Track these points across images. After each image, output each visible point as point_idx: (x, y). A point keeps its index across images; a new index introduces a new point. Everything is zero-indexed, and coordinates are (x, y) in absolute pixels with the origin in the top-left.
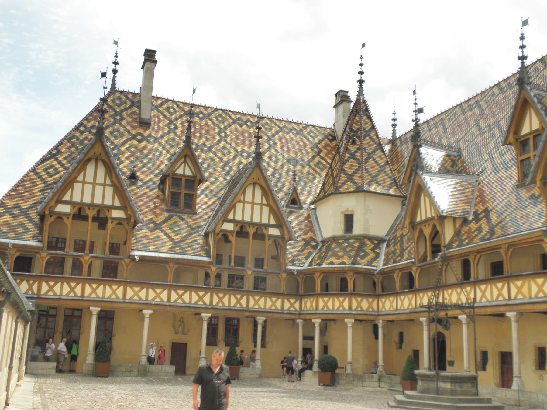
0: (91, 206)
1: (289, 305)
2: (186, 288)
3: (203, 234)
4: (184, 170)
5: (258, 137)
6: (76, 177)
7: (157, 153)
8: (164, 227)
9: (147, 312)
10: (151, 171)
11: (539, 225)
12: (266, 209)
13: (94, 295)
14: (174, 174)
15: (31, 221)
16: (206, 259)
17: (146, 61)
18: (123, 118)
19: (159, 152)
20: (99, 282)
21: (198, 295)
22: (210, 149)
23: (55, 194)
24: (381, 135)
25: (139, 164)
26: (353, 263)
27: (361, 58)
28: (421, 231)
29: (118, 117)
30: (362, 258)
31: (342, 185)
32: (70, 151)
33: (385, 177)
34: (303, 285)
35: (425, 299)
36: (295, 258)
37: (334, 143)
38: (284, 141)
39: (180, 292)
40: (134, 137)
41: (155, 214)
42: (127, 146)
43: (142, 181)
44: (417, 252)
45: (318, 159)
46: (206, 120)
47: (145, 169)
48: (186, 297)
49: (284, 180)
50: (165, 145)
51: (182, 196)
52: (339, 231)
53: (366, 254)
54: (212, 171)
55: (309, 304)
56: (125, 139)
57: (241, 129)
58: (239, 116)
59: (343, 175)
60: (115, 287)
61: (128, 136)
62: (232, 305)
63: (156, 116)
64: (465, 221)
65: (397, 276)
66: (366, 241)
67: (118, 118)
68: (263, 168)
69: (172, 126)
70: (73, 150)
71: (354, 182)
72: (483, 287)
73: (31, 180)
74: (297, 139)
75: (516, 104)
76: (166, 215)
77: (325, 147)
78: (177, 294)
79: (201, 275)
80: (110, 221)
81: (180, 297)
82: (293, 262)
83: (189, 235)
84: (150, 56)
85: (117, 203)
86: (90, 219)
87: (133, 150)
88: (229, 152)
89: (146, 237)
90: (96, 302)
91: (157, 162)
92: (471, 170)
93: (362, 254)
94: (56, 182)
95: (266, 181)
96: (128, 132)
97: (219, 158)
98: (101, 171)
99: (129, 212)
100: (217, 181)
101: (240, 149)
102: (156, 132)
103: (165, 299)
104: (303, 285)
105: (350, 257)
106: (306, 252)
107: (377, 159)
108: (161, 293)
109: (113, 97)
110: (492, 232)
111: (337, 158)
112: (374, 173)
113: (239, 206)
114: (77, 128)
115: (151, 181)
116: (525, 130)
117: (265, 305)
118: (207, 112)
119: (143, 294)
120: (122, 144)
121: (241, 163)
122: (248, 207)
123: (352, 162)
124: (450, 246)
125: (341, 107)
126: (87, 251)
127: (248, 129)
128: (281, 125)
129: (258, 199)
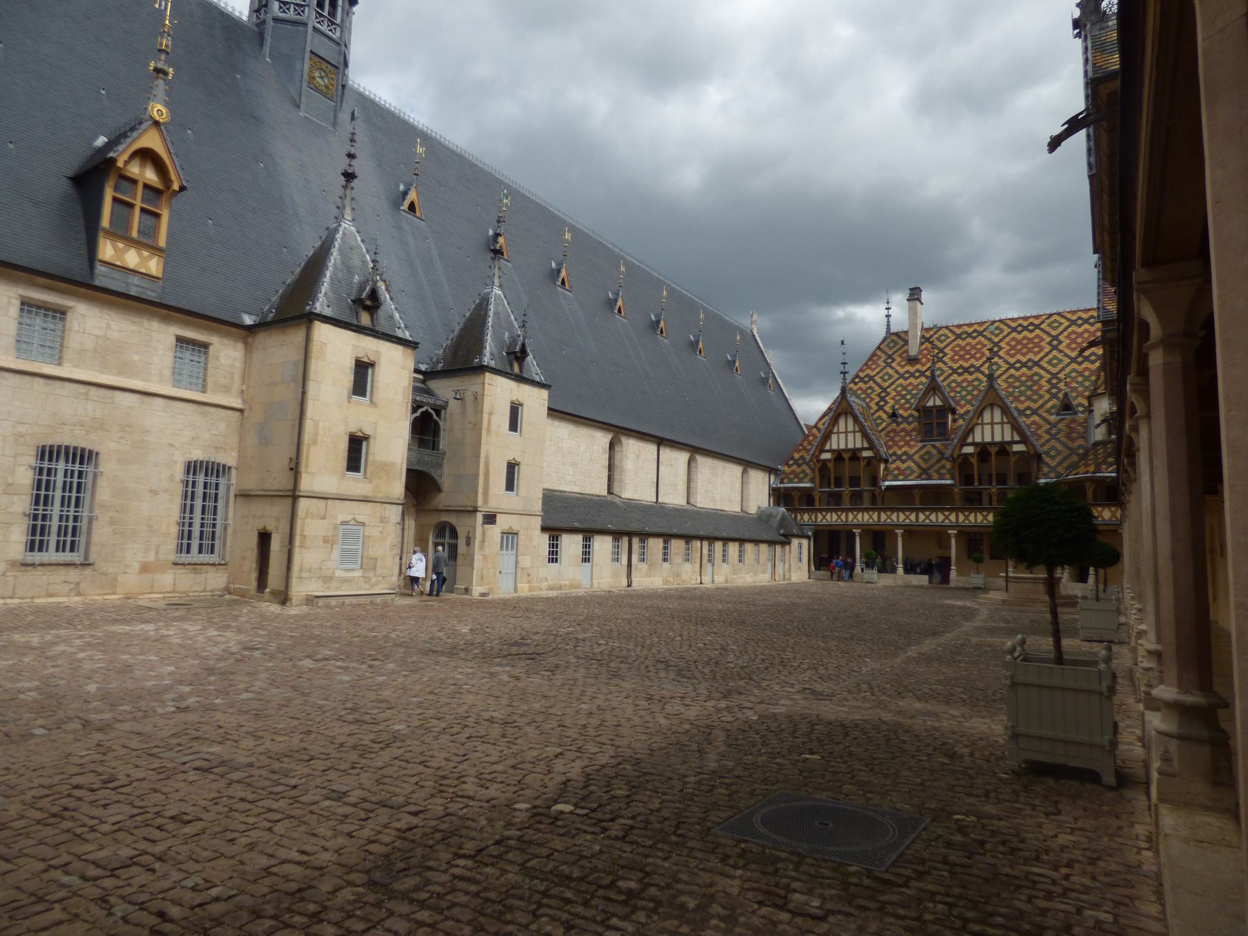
0: (847, 450)
2: (932, 510)
4: (934, 402)
9: (899, 532)
12: (1007, 428)
14: (924, 407)
15: (810, 467)
16: (949, 482)
18: (894, 360)
36: (1053, 469)
38: (1073, 336)
40: (902, 376)
41: (910, 447)
43: (902, 416)
48: (933, 517)
58: (1020, 322)
76: (920, 445)
81: (927, 517)
85: (866, 445)
90: (857, 526)
95: (1002, 400)
96: (897, 372)
113: (978, 430)
115: (911, 415)
119: (894, 517)
122: (988, 428)
128: (1074, 318)
129: (997, 418)
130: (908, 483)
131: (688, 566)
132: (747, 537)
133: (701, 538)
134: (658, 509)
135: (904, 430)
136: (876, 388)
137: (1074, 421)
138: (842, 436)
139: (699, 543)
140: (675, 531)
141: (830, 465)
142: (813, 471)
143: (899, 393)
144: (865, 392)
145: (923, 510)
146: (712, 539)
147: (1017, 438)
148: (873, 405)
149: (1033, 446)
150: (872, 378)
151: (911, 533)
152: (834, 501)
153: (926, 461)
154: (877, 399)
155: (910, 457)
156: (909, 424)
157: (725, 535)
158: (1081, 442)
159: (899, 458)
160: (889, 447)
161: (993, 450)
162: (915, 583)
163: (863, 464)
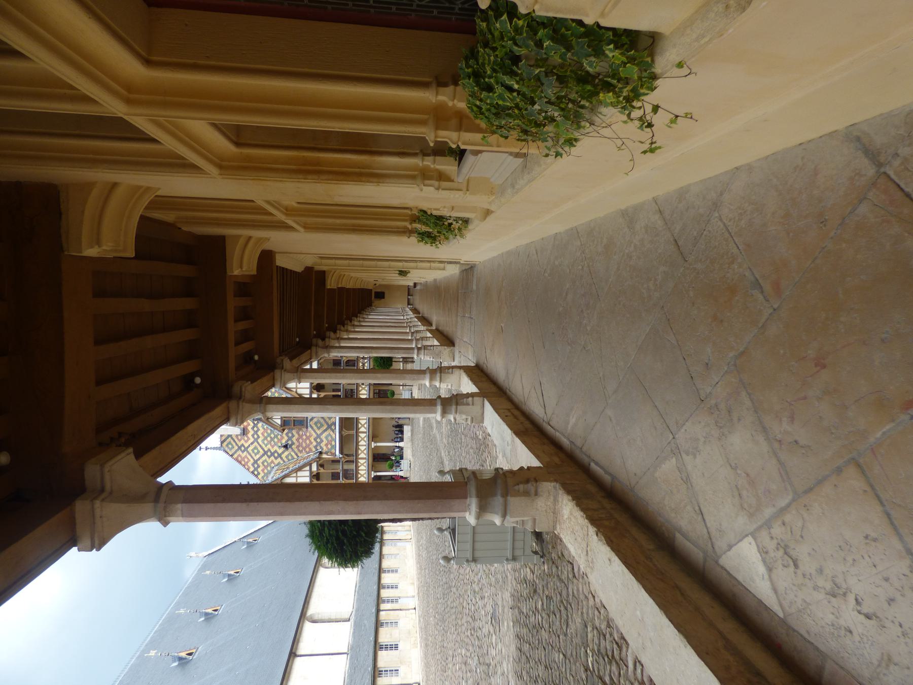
9: (373, 445)
14: (281, 426)
18: (243, 445)
25: (276, 440)
40: (256, 440)
41: (310, 436)
61: (256, 443)
76: (310, 429)
81: (363, 426)
85: (308, 468)
89: (326, 445)
96: (252, 443)
113: (300, 391)
115: (287, 434)
119: (362, 448)
131: (401, 623)
132: (377, 566)
133: (378, 610)
134: (353, 652)
135: (297, 440)
136: (264, 458)
139: (382, 613)
140: (372, 638)
143: (270, 442)
144: (266, 467)
145: (357, 429)
146: (379, 600)
148: (276, 462)
150: (256, 462)
151: (374, 436)
153: (322, 425)
154: (272, 458)
155: (318, 436)
156: (293, 436)
157: (376, 587)
159: (319, 444)
160: (311, 450)
163: (322, 470)
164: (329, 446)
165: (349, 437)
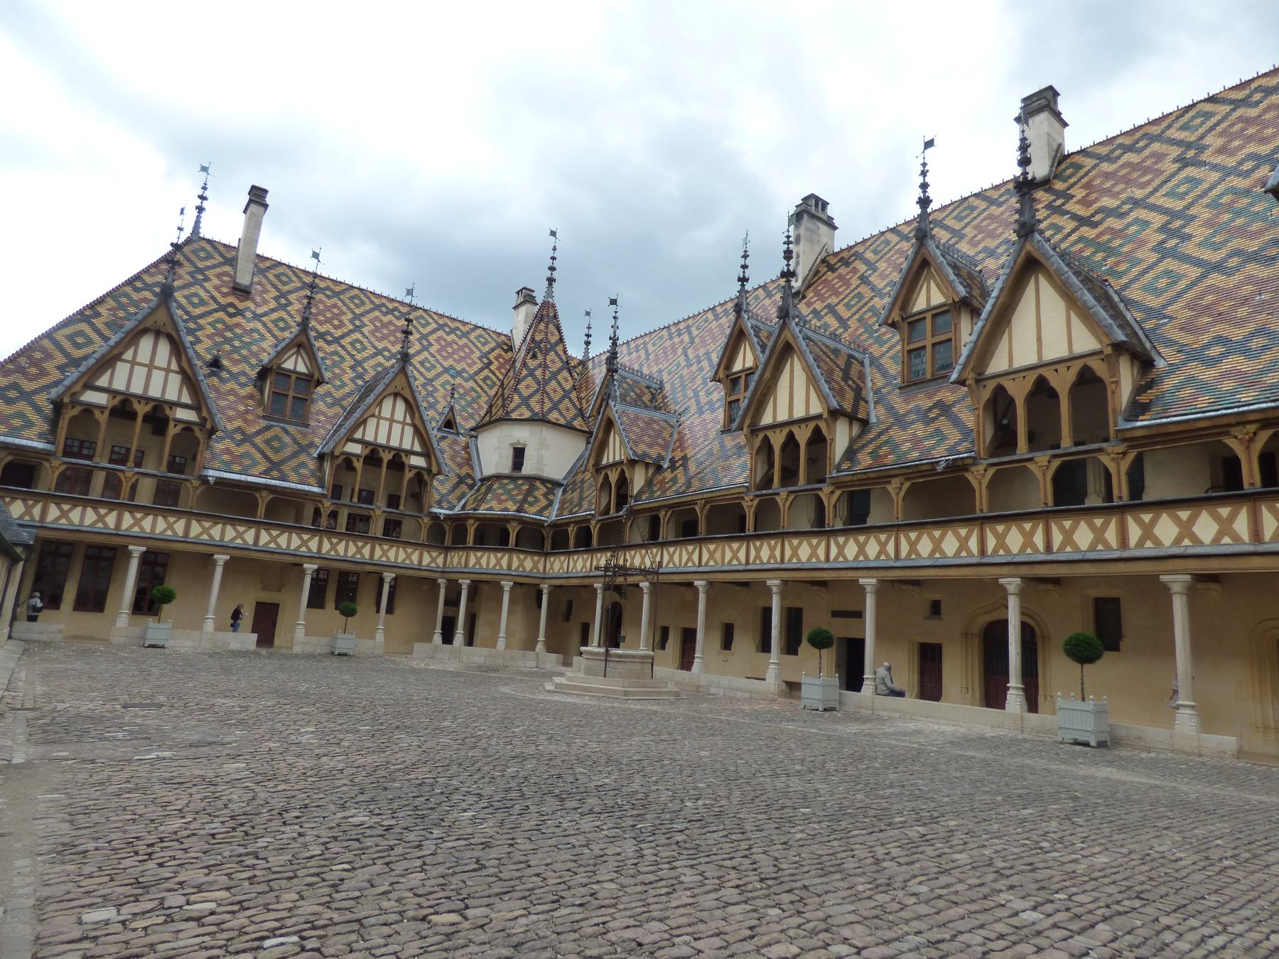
0: (144, 399)
1: (429, 560)
3: (315, 455)
4: (296, 364)
5: (407, 333)
6: (122, 353)
7: (256, 336)
8: (258, 440)
9: (221, 558)
10: (245, 359)
11: (741, 480)
12: (409, 431)
13: (136, 529)
14: (279, 367)
16: (316, 490)
17: (250, 201)
18: (207, 279)
19: (260, 334)
20: (146, 510)
21: (301, 539)
22: (337, 340)
23: (83, 374)
24: (571, 352)
25: (227, 347)
26: (518, 511)
27: (554, 249)
28: (606, 476)
29: (199, 275)
30: (531, 505)
31: (513, 411)
32: (114, 315)
33: (570, 405)
34: (449, 533)
35: (602, 559)
37: (510, 354)
38: (443, 343)
39: (275, 533)
40: (223, 308)
41: (246, 421)
42: (210, 319)
43: (229, 372)
44: (598, 502)
45: (486, 372)
46: (335, 300)
47: (236, 356)
48: (283, 540)
49: (439, 395)
50: (270, 325)
51: (290, 398)
52: (506, 468)
53: (537, 500)
54: (337, 371)
55: (456, 559)
56: (208, 309)
57: (385, 319)
58: (384, 301)
59: (516, 397)
60: (172, 520)
62: (349, 554)
63: (259, 283)
64: (659, 468)
65: (572, 531)
66: (538, 484)
67: (200, 277)
68: (410, 374)
69: (283, 301)
70: (121, 314)
71: (530, 409)
72: (672, 549)
73: (44, 350)
74: (460, 343)
75: (731, 334)
76: (263, 423)
77: (497, 358)
78: (270, 535)
79: (309, 512)
80: (172, 424)
81: (274, 539)
82: (439, 504)
83: (294, 455)
84: (258, 196)
85: (186, 399)
86: (140, 419)
87: (219, 326)
88: (365, 348)
89: (228, 451)
91: (254, 348)
92: (672, 407)
93: (530, 499)
94: (86, 358)
95: (412, 392)
97: (349, 353)
98: (164, 349)
99: (205, 414)
100: (344, 385)
101: (380, 346)
102: (257, 305)
103: (251, 541)
104: (449, 533)
105: (515, 503)
106: (458, 492)
107: (563, 382)
108: (244, 532)
109: (196, 246)
110: (689, 485)
111: (511, 374)
112: (556, 399)
113: (372, 423)
114: (130, 282)
116: (737, 367)
117: (396, 557)
118: (337, 289)
119: (216, 532)
120: (202, 316)
121: (380, 364)
122: (384, 425)
123: (529, 380)
124: (638, 497)
125: (523, 310)
126: (131, 464)
127: (395, 321)
128: (441, 322)
130: (250, 479)
137: (455, 442)
138: (140, 372)
141: (103, 418)
142: (54, 422)
145: (268, 527)
147: (417, 448)
149: (438, 464)
152: (74, 486)
153: (277, 451)
158: (464, 471)
159: (229, 435)
161: (386, 457)
162: (235, 646)
164: (226, 457)
165: (251, 507)
